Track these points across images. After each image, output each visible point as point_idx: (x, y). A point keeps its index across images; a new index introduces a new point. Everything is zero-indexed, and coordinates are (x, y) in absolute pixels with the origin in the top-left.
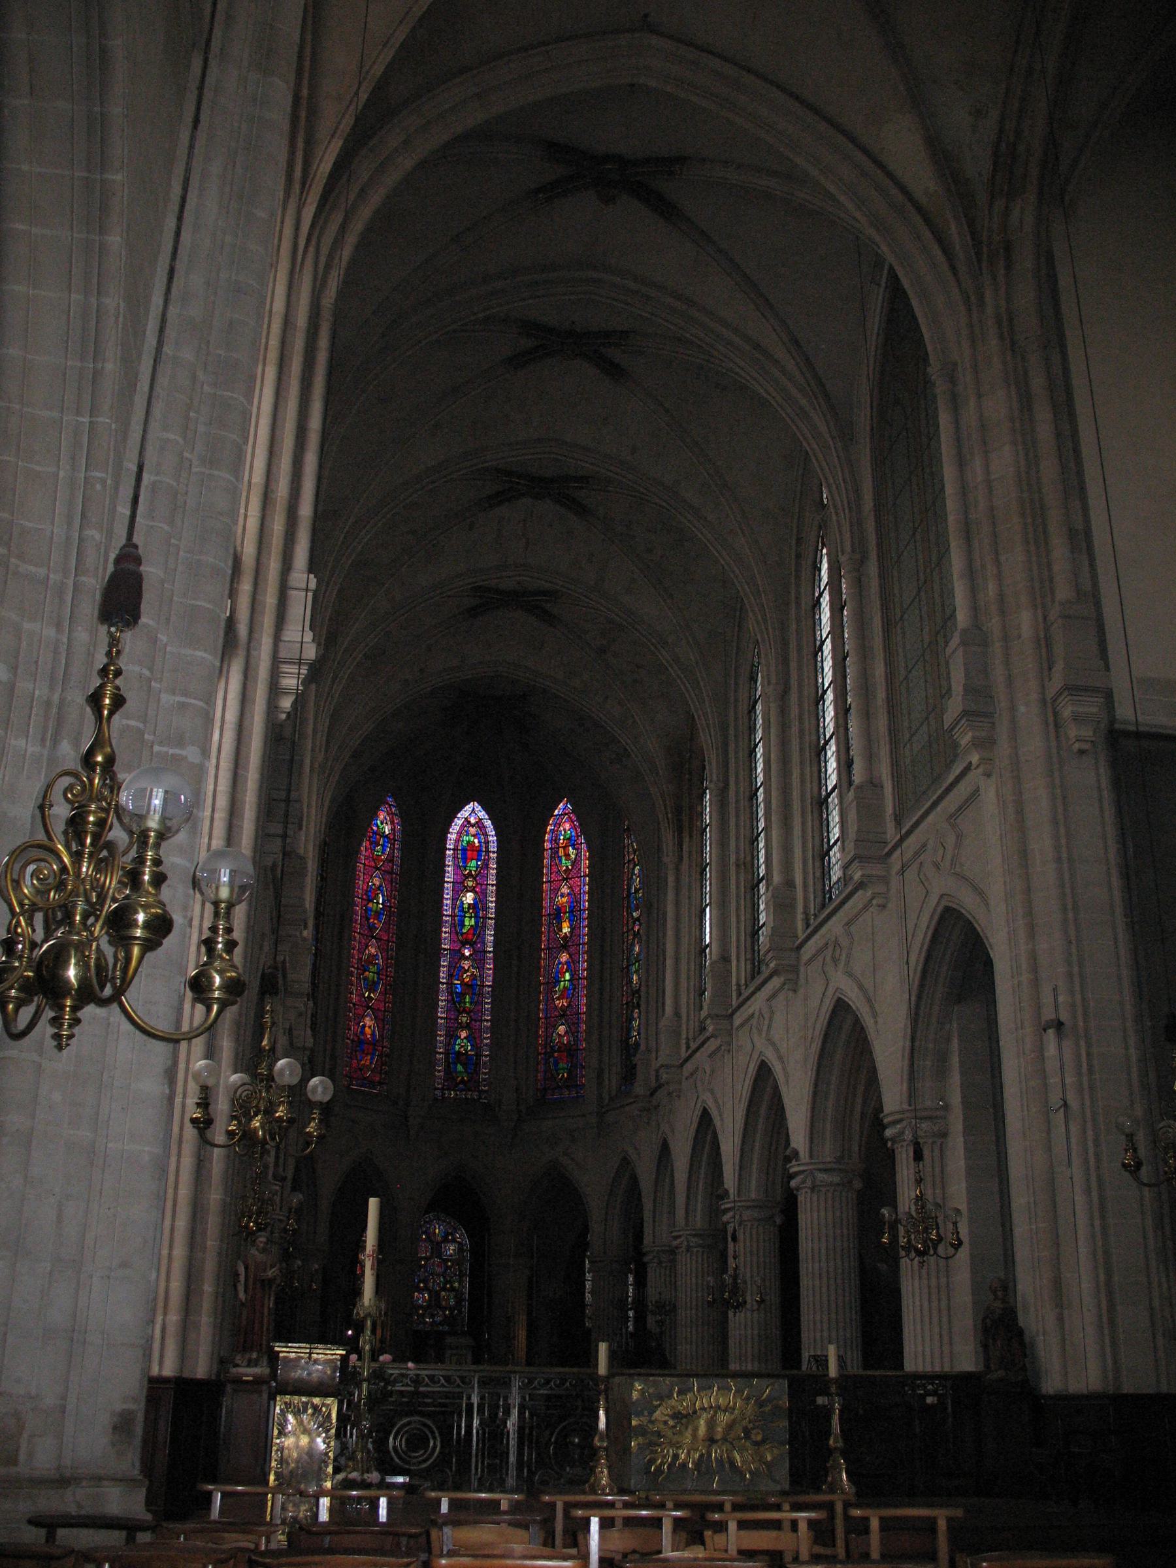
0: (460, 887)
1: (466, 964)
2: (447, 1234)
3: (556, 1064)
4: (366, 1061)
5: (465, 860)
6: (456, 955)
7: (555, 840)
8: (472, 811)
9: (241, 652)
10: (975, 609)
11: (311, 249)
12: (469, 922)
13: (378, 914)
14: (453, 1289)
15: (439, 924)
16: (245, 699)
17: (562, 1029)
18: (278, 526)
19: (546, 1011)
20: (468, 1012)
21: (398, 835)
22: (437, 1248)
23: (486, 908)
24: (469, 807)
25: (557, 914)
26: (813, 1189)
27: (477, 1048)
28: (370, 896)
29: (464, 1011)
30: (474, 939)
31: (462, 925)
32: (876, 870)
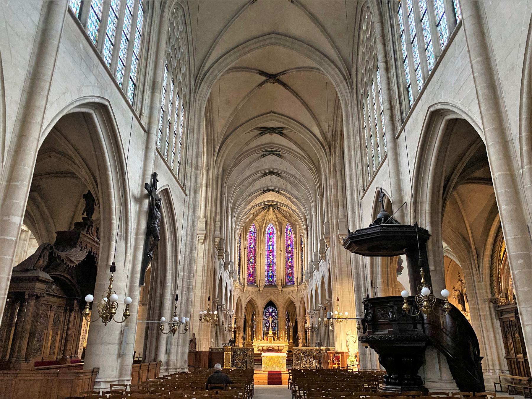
0: (268, 241)
1: (270, 257)
7: (287, 230)
8: (271, 225)
9: (208, 238)
12: (271, 248)
13: (252, 248)
16: (209, 245)
18: (213, 215)
22: (270, 314)
24: (270, 225)
25: (288, 246)
32: (324, 255)
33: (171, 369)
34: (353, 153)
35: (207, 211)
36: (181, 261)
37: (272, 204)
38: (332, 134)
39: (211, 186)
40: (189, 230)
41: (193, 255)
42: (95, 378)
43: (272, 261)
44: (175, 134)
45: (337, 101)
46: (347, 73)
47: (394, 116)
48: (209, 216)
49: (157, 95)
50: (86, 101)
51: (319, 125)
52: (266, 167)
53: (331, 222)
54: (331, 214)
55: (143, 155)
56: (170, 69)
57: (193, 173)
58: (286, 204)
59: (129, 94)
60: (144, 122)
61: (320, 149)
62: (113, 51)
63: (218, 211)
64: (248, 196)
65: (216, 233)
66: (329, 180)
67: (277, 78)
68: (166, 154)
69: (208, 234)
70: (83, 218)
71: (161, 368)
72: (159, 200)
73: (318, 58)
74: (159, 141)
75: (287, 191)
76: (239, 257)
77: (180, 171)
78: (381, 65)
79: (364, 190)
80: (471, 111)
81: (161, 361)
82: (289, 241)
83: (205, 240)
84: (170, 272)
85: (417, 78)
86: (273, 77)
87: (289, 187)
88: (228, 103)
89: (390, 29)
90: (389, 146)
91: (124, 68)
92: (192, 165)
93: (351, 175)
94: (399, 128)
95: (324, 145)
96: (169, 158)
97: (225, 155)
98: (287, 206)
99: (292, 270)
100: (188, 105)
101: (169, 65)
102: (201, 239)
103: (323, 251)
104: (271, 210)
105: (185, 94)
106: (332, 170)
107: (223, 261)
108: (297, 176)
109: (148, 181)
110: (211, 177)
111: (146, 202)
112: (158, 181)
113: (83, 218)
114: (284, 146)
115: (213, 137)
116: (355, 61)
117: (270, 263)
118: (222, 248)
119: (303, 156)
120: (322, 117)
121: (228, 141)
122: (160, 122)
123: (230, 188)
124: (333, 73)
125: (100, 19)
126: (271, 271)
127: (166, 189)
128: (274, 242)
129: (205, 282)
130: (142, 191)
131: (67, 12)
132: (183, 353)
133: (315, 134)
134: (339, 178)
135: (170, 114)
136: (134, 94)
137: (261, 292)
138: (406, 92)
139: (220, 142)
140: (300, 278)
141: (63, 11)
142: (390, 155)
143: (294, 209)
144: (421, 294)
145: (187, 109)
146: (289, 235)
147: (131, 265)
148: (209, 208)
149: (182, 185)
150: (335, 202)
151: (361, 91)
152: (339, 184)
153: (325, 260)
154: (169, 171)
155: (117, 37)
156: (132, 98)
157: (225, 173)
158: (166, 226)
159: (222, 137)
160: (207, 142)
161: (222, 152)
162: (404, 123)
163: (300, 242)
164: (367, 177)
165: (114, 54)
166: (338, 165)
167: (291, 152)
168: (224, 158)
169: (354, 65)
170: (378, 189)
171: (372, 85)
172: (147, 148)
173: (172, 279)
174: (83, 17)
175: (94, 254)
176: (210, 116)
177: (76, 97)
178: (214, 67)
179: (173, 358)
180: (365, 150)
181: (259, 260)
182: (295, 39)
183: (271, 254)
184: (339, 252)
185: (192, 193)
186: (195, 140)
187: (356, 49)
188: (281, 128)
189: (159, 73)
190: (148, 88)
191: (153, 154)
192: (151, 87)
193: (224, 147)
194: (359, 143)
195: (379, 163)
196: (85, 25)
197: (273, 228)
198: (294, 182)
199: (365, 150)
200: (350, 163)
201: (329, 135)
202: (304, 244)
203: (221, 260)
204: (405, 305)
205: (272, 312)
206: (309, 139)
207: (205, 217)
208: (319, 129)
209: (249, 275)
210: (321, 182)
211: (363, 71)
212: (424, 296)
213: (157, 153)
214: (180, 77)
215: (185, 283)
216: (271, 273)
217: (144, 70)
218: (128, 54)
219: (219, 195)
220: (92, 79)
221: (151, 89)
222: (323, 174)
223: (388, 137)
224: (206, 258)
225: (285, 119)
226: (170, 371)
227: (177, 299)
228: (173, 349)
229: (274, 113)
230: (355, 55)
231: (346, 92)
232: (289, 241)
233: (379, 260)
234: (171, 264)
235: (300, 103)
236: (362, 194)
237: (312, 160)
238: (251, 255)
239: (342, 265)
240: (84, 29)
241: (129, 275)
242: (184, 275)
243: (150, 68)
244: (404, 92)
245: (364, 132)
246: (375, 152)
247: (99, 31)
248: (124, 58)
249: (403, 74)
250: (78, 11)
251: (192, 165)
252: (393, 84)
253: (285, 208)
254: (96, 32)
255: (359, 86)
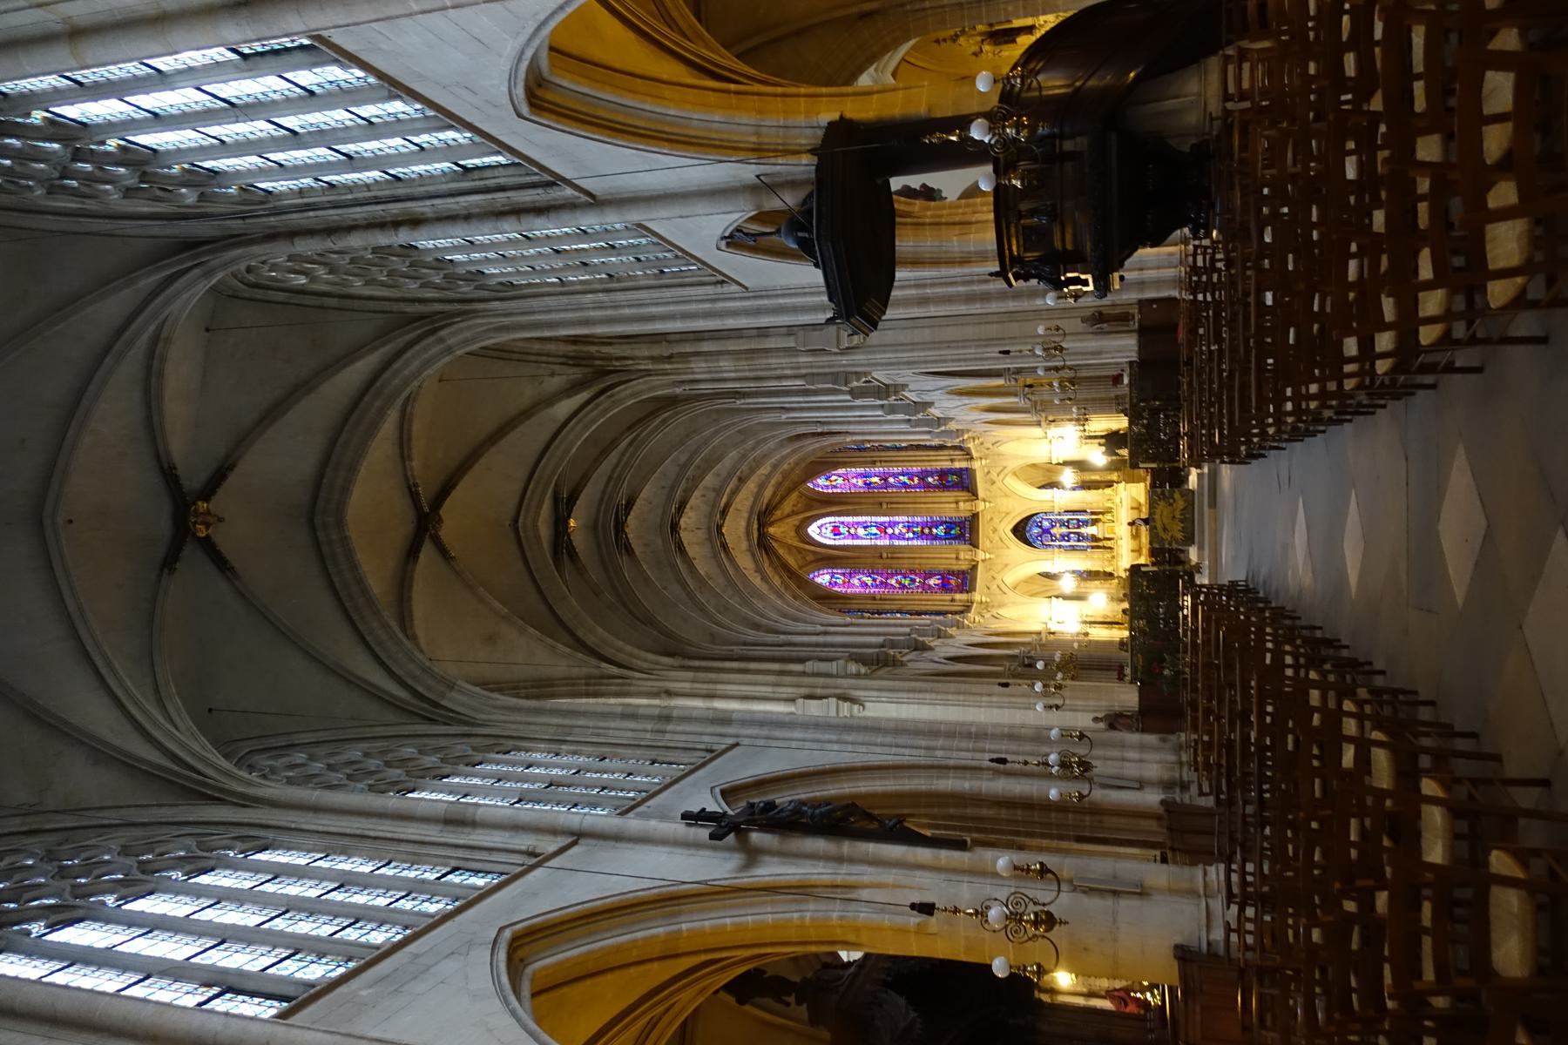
1: (897, 531)
2: (1038, 526)
3: (949, 482)
4: (953, 582)
5: (840, 534)
6: (892, 537)
7: (827, 487)
8: (813, 530)
9: (847, 691)
10: (796, 377)
11: (655, 672)
12: (874, 530)
13: (874, 580)
14: (1068, 522)
15: (876, 547)
16: (866, 689)
17: (930, 480)
18: (787, 679)
19: (920, 488)
20: (923, 528)
21: (830, 571)
22: (1047, 531)
23: (866, 522)
25: (868, 485)
26: (1032, 394)
27: (942, 523)
28: (864, 585)
29: (922, 531)
30: (882, 528)
31: (875, 534)
32: (892, 389)
33: (1181, 776)
34: (627, 311)
35: (777, 695)
36: (906, 757)
37: (756, 526)
38: (574, 365)
39: (711, 686)
40: (827, 737)
41: (892, 725)
42: (1199, 953)
43: (909, 527)
44: (578, 772)
45: (484, 353)
46: (418, 328)
47: (537, 204)
48: (790, 690)
49: (480, 814)
50: (505, 979)
51: (550, 400)
52: (659, 542)
53: (807, 367)
54: (783, 369)
55: (638, 847)
56: (411, 785)
57: (679, 728)
58: (755, 490)
59: (479, 881)
60: (549, 845)
61: (613, 399)
62: (370, 920)
63: (776, 666)
64: (738, 592)
65: (835, 672)
66: (693, 373)
67: (426, 509)
68: (631, 795)
69: (838, 691)
70: (799, 1003)
71: (1178, 799)
72: (752, 805)
73: (378, 403)
74: (599, 811)
75: (721, 487)
76: (898, 615)
77: (672, 760)
78: (403, 237)
79: (723, 282)
80: (536, 14)
81: (1163, 802)
82: (854, 481)
83: (853, 700)
84: (935, 782)
85: (442, 145)
86: (425, 523)
87: (709, 480)
88: (491, 639)
89: (311, 214)
90: (614, 220)
91: (414, 895)
92: (658, 731)
93: (686, 316)
94: (569, 192)
95: (602, 386)
96: (640, 788)
97: (628, 648)
98: (762, 487)
99: (931, 474)
100: (503, 741)
101: (397, 788)
102: (851, 710)
103: (884, 391)
104: (771, 530)
105: (474, 749)
106: (667, 366)
107: (907, 654)
108: (683, 458)
109: (703, 833)
110: (687, 685)
111: (756, 837)
112: (704, 810)
113: (799, 1003)
114: (604, 492)
115: (581, 679)
116: (387, 306)
117: (914, 533)
118: (875, 657)
119: (630, 444)
120: (528, 393)
121: (590, 640)
122: (548, 808)
123: (713, 638)
124: (416, 363)
125: (289, 952)
126: (934, 530)
127: (723, 792)
128: (857, 523)
129: (961, 697)
130: (728, 849)
131: (289, 1021)
132: (1142, 747)
133: (572, 411)
134: (688, 348)
135: (525, 786)
136: (479, 872)
137: (988, 556)
138: (476, 174)
139: (593, 661)
140: (952, 452)
141: (283, 1029)
142: (635, 216)
143: (769, 469)
144: (986, 141)
145: (511, 743)
146: (840, 481)
147: (918, 873)
148: (769, 689)
149: (709, 756)
150: (752, 359)
151: (466, 289)
152: (706, 347)
153: (904, 386)
154: (676, 787)
155: (335, 911)
156: (490, 876)
157: (675, 649)
158: (818, 794)
159: (580, 655)
160: (596, 695)
161: (620, 657)
162: (556, 180)
163: (858, 454)
164: (689, 274)
165: (380, 918)
166: (657, 351)
167: (619, 477)
168: (636, 651)
169: (396, 307)
170: (723, 247)
171: (451, 261)
172: (617, 838)
173: (954, 778)
174: (290, 991)
175: (889, 975)
176: (526, 688)
177: (497, 1003)
178: (400, 673)
179: (1153, 771)
180: (619, 280)
181: (906, 561)
182: (326, 460)
183: (890, 531)
184: (884, 347)
185: (731, 730)
186: (591, 724)
187: (356, 303)
188: (556, 498)
189: (420, 810)
190: (463, 836)
191: (633, 824)
192: (460, 829)
193: (608, 652)
194: (600, 295)
195: (654, 244)
196: (311, 985)
197: (822, 526)
198: (699, 467)
199: (619, 280)
200: (652, 318)
201: (575, 373)
202: (863, 442)
203: (905, 659)
204: (1014, 182)
205: (1040, 527)
206: (586, 427)
207: (792, 700)
208: (560, 399)
209: (945, 587)
210: (703, 395)
211: (413, 285)
212: (994, 136)
213: (631, 815)
214: (431, 760)
215: (964, 744)
216: (940, 531)
217: (416, 846)
218: (377, 887)
219: (735, 665)
220: (449, 967)
221: (467, 830)
222: (678, 390)
223: (590, 221)
224: (900, 695)
225: (533, 492)
226: (1185, 778)
227: (1003, 761)
228: (1131, 770)
229: (516, 520)
230: (371, 305)
231: (469, 328)
232: (854, 481)
233: (904, 243)
234: (916, 781)
235: (493, 450)
236: (735, 288)
237: (640, 420)
238: (893, 582)
239: (916, 340)
240: (318, 988)
241: (943, 876)
242: (942, 749)
243: (410, 831)
244: (473, 180)
245: (572, 283)
246: (626, 255)
247: (321, 955)
248: (388, 895)
249: (427, 181)
250: (276, 1004)
251: (658, 731)
252: (455, 206)
253: (768, 493)
254: (324, 960)
255: (450, 295)
